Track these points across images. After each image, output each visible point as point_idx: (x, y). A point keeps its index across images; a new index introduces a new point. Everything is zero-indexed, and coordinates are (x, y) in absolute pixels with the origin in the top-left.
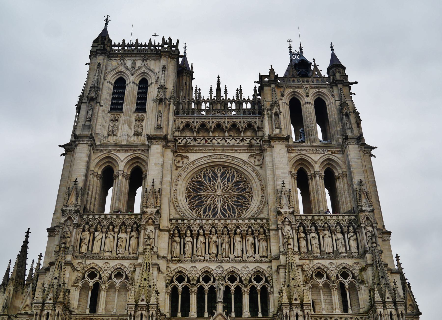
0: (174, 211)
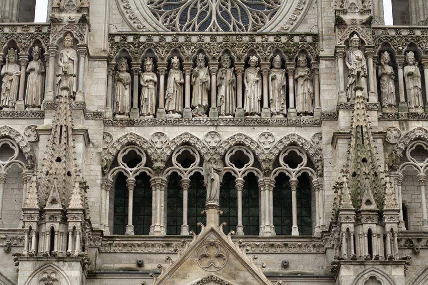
0: (119, 17)
